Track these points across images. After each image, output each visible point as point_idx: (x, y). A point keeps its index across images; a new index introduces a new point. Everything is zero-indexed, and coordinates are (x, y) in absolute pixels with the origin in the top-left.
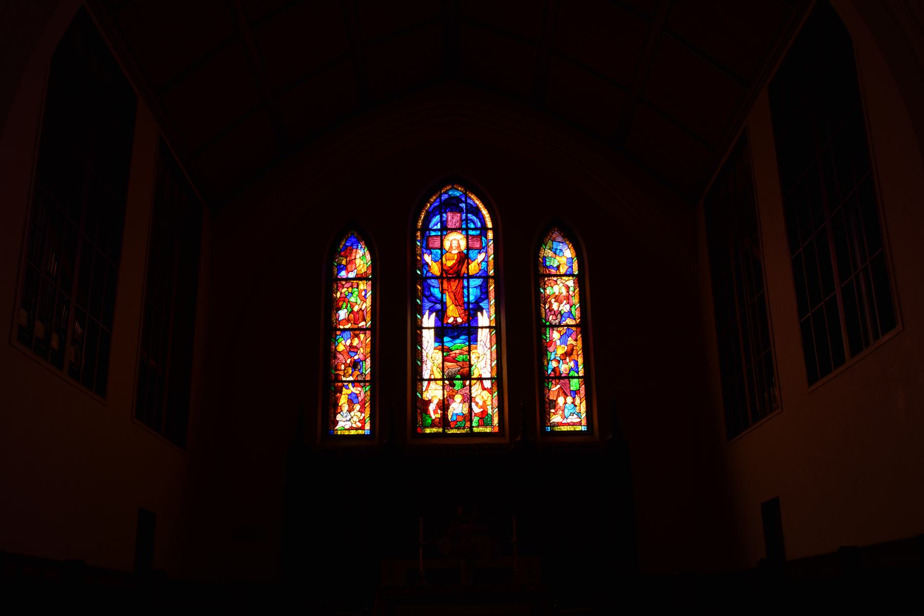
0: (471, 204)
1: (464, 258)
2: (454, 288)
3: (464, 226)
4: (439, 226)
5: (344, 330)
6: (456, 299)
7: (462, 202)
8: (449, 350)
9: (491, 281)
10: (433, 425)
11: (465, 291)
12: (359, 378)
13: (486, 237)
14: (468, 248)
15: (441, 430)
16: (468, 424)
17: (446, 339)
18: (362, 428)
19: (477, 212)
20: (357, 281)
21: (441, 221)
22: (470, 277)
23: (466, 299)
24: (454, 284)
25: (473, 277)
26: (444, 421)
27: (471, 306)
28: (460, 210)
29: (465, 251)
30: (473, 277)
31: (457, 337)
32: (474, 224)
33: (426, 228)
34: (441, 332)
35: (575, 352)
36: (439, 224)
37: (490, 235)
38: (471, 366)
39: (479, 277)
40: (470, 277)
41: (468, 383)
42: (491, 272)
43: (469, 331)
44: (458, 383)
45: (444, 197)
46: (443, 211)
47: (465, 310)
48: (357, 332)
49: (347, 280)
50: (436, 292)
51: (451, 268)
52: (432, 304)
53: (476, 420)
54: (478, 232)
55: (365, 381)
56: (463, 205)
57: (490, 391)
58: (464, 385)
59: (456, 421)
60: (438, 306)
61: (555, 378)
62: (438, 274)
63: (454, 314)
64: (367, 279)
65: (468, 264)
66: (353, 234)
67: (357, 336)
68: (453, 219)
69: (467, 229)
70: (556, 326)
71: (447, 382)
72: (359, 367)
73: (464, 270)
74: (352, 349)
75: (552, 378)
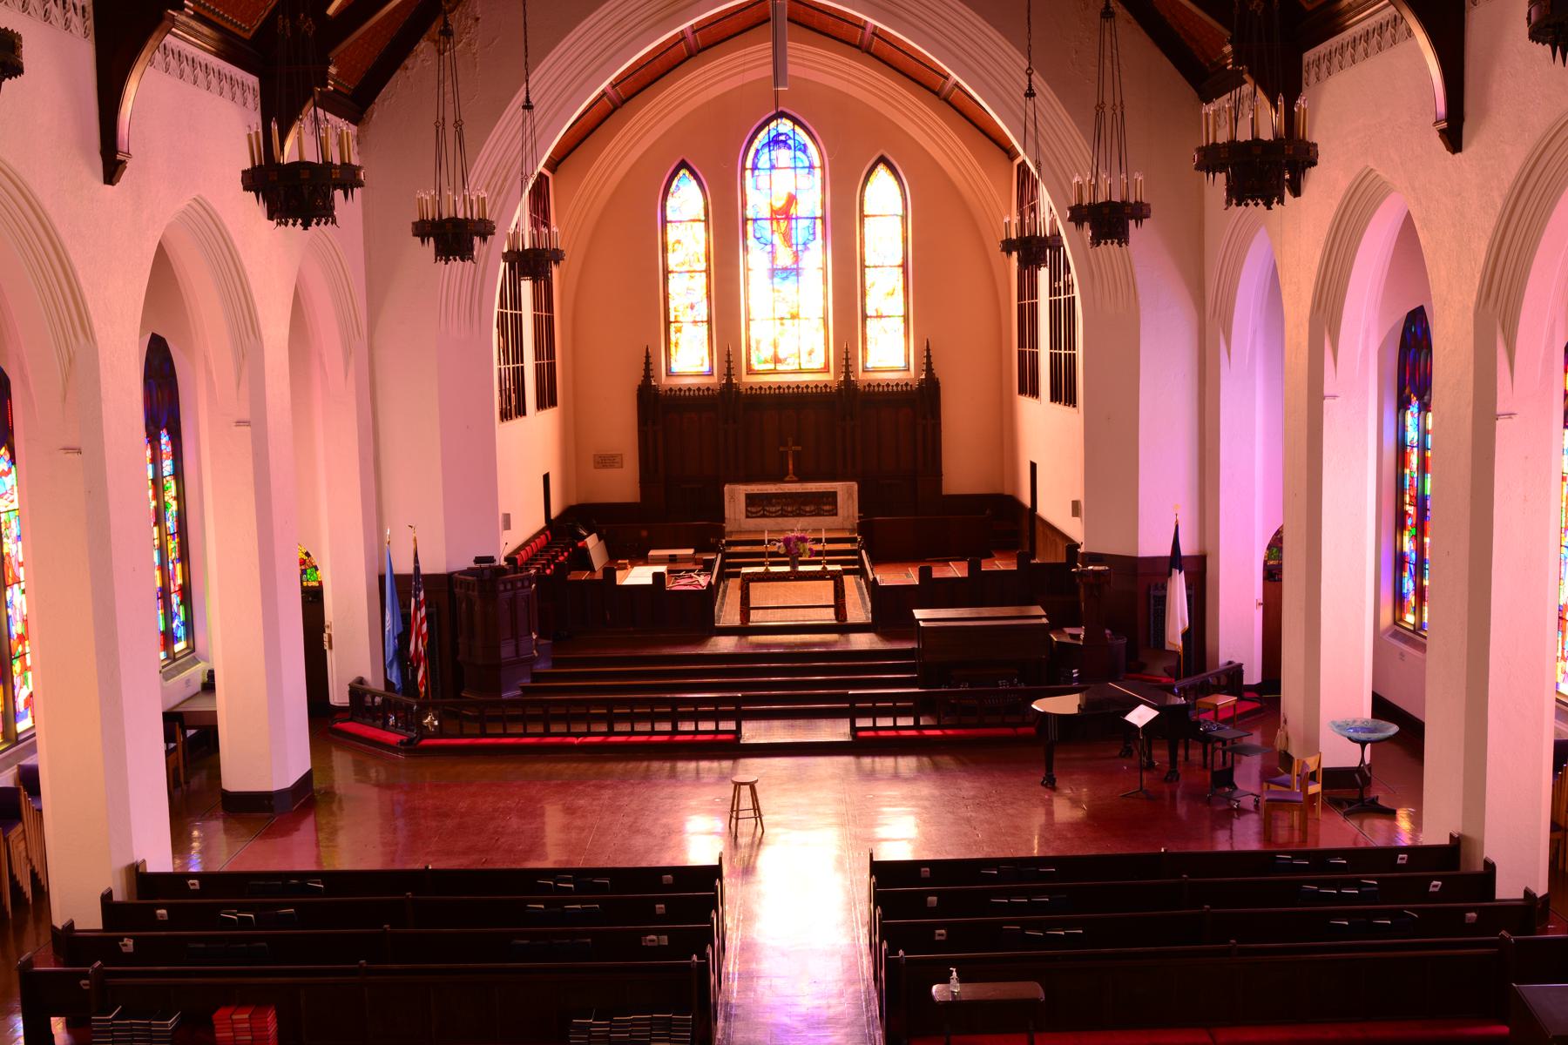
0: (800, 144)
1: (792, 199)
2: (783, 231)
3: (793, 166)
4: (768, 166)
5: (681, 272)
6: (785, 240)
7: (790, 138)
8: (778, 291)
9: (819, 222)
10: (766, 362)
11: (794, 232)
12: (697, 320)
13: (813, 176)
14: (796, 189)
15: (771, 366)
16: (797, 361)
17: (776, 280)
18: (702, 365)
19: (804, 149)
20: (692, 223)
21: (770, 160)
22: (797, 218)
23: (794, 241)
24: (783, 224)
25: (801, 218)
26: (777, 360)
27: (800, 248)
28: (790, 148)
29: (794, 193)
30: (801, 218)
31: (787, 277)
32: (802, 162)
33: (755, 168)
34: (773, 272)
35: (896, 292)
36: (769, 162)
37: (818, 172)
38: (798, 307)
39: (807, 218)
40: (797, 218)
41: (796, 321)
42: (819, 213)
43: (795, 271)
44: (788, 322)
45: (773, 133)
46: (772, 148)
47: (794, 253)
48: (693, 274)
49: (680, 222)
50: (767, 234)
51: (780, 209)
52: (763, 246)
53: (804, 357)
54: (807, 170)
55: (702, 322)
56: (791, 142)
57: (817, 330)
58: (794, 325)
59: (785, 359)
60: (769, 248)
61: (877, 317)
62: (769, 216)
63: (785, 257)
64: (699, 221)
65: (796, 203)
66: (684, 174)
67: (692, 277)
68: (783, 156)
69: (795, 168)
70: (879, 266)
71: (779, 321)
72: (695, 309)
73: (792, 211)
74: (689, 291)
75: (875, 317)
